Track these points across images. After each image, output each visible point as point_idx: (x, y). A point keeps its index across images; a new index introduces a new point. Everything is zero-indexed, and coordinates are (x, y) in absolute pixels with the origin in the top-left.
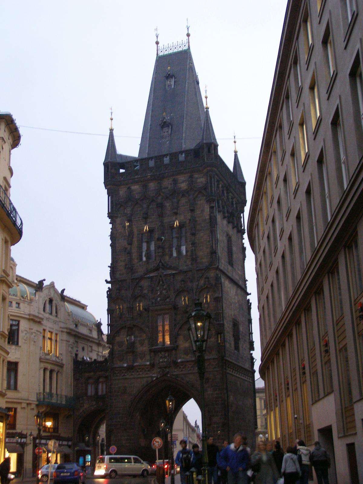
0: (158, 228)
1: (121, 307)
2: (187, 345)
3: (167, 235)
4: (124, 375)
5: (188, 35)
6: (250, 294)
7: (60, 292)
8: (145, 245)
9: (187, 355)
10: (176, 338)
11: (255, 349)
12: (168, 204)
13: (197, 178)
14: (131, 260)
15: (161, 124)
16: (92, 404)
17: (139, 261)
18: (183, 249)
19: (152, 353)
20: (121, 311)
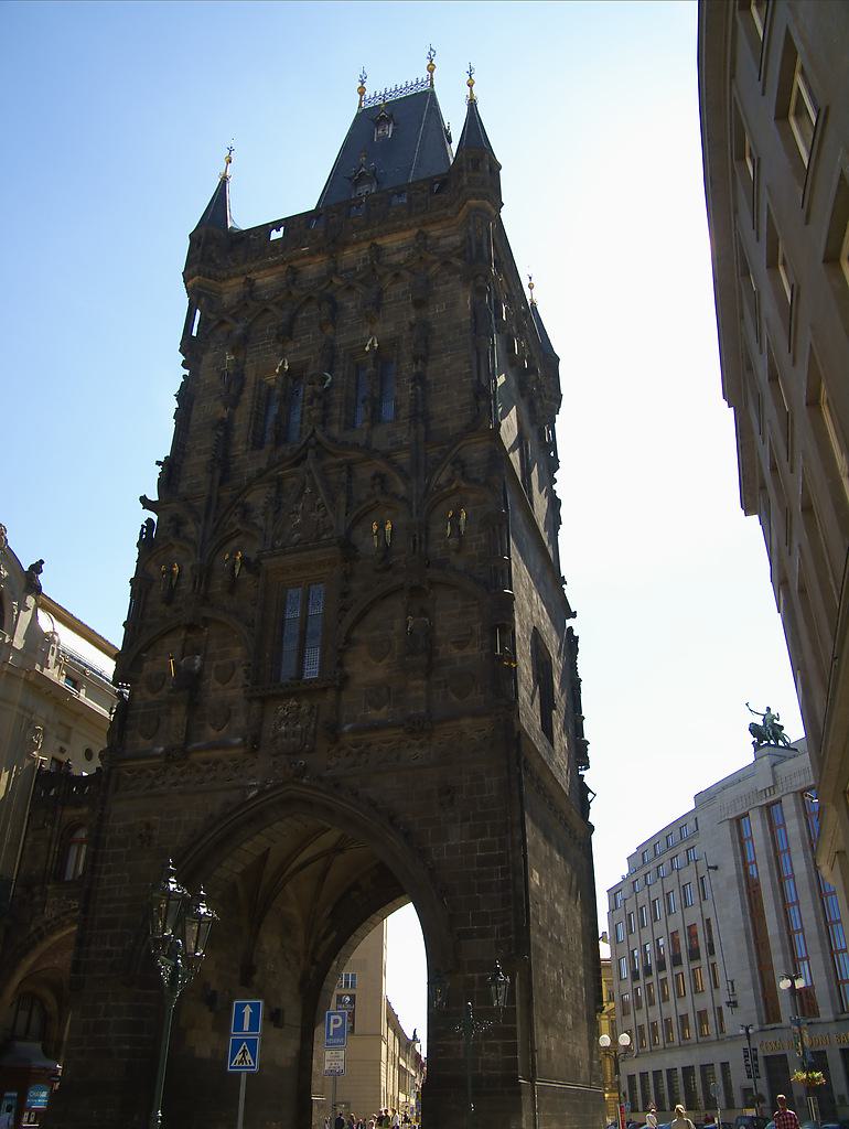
0: (315, 362)
1: (176, 569)
2: (379, 672)
3: (341, 375)
4: (151, 787)
5: (431, 68)
6: (574, 615)
7: (26, 569)
8: (274, 410)
9: (378, 708)
10: (340, 651)
11: (590, 764)
12: (350, 304)
13: (438, 238)
14: (225, 442)
15: (350, 179)
16: (70, 905)
17: (250, 446)
18: (388, 410)
19: (256, 705)
20: (174, 583)
